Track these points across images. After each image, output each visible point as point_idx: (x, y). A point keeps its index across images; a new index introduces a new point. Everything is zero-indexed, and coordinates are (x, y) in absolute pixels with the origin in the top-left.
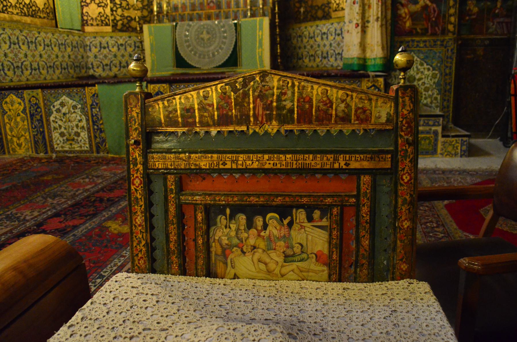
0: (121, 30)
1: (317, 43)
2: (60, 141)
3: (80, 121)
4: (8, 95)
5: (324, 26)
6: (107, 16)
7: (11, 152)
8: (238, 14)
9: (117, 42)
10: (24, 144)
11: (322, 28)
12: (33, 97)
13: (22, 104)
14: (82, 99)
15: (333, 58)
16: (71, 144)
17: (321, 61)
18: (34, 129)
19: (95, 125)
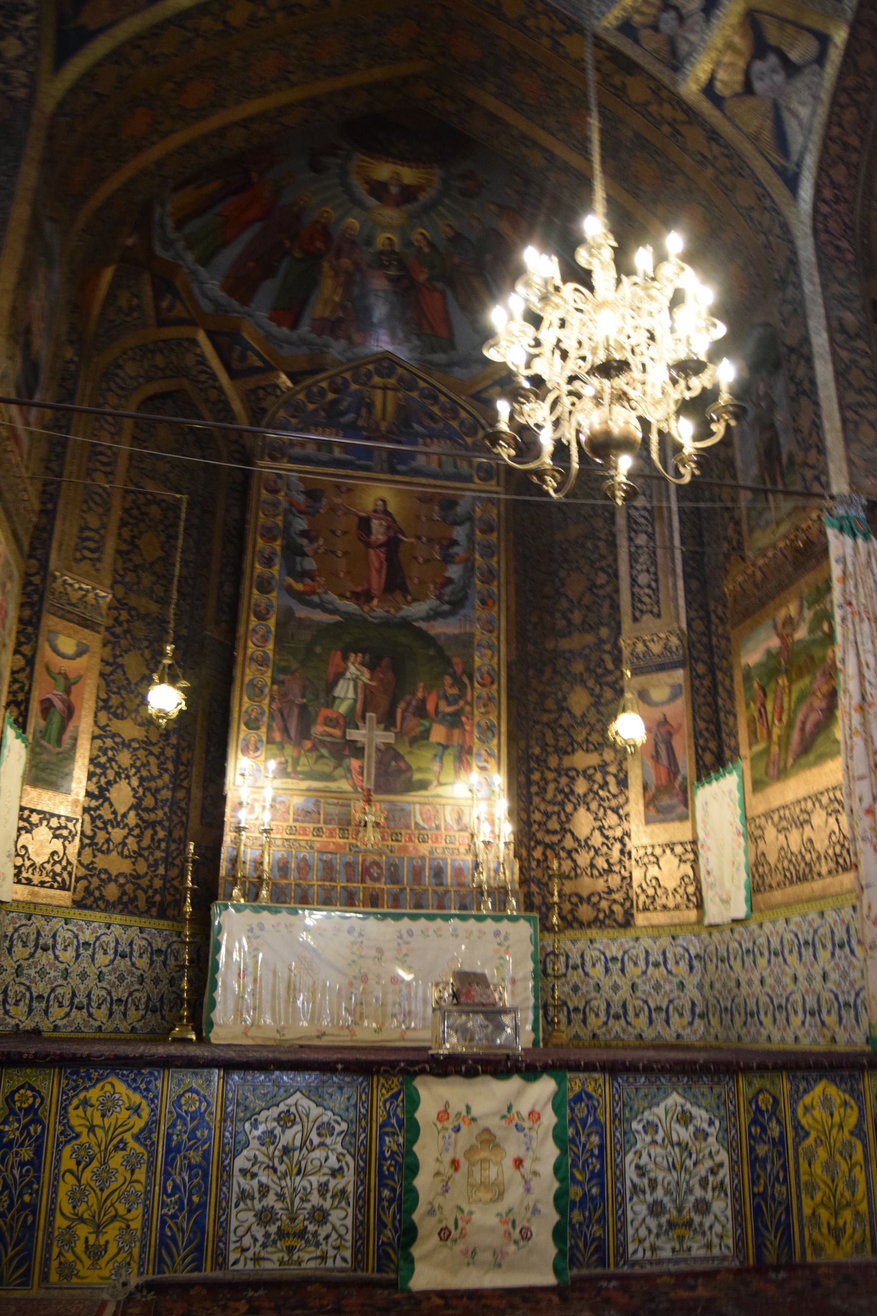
0: (78, 904)
1: (592, 982)
2: (255, 1240)
3: (336, 1173)
4: (98, 1080)
5: (609, 943)
6: (69, 863)
7: (54, 1277)
8: (446, 900)
9: (76, 936)
10: (112, 1249)
11: (608, 946)
12: (191, 1090)
13: (145, 1112)
14: (355, 1106)
15: (643, 1019)
16: (290, 1250)
17: (605, 1023)
18: (169, 1196)
19: (386, 1186)
